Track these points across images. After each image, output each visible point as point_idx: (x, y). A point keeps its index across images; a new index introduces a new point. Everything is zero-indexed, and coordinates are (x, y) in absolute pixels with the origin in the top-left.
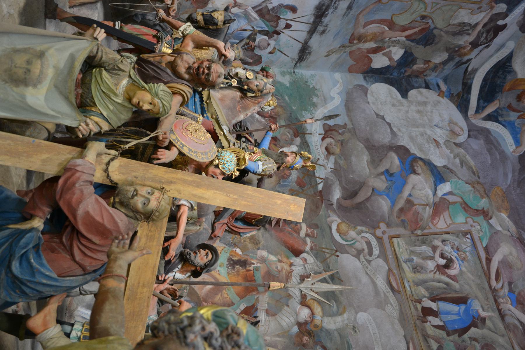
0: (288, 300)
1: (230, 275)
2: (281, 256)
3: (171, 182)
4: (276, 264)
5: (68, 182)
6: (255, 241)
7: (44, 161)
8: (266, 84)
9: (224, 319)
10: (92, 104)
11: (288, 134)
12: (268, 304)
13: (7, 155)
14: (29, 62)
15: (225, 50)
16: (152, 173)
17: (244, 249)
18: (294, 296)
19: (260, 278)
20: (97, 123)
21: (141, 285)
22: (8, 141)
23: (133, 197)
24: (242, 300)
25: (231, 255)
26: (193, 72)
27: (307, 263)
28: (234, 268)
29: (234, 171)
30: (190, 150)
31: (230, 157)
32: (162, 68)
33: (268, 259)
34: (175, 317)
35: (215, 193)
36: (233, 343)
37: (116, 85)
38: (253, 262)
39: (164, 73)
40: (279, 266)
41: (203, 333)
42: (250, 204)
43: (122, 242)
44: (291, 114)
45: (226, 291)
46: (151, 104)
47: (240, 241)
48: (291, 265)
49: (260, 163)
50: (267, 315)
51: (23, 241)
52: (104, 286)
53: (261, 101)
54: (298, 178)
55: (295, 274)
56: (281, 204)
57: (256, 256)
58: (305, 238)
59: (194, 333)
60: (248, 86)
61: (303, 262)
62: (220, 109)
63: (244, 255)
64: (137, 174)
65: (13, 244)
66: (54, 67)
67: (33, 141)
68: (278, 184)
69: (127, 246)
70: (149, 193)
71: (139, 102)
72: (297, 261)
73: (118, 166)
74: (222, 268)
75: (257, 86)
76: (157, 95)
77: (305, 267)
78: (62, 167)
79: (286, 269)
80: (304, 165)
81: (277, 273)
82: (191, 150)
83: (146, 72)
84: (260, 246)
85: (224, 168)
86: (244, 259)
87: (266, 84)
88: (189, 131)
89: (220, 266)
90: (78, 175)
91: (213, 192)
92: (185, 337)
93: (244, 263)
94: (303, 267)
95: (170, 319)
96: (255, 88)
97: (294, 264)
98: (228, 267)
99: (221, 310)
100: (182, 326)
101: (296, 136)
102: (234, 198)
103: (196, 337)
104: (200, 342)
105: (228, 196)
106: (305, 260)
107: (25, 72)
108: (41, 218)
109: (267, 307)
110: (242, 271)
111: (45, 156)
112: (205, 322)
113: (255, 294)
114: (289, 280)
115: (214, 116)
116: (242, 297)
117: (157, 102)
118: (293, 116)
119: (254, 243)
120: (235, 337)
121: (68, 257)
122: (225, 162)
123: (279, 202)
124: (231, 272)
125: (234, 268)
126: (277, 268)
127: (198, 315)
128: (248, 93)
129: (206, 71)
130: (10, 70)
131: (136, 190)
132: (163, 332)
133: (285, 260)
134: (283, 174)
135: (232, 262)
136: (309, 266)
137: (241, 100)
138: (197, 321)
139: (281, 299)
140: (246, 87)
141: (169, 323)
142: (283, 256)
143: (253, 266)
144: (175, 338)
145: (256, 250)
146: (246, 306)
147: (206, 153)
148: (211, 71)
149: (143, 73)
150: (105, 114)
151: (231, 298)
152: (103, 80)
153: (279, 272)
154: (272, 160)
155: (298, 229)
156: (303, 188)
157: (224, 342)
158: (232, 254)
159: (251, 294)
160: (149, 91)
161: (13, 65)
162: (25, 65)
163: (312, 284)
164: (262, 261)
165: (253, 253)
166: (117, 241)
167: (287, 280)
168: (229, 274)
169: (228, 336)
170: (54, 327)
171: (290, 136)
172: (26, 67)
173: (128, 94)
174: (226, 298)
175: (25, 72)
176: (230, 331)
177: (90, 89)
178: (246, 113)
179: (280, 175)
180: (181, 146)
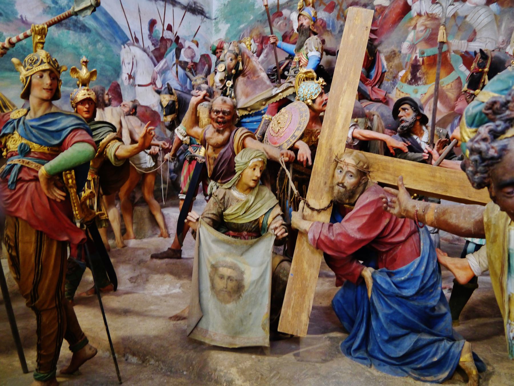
0: (459, 17)
1: (427, 82)
2: (409, 27)
3: (330, 149)
5: (330, 246)
6: (391, 56)
7: (310, 266)
8: (229, 51)
9: (476, 115)
10: (256, 223)
11: (279, 23)
12: (461, 39)
13: (305, 296)
14: (222, 277)
15: (199, 95)
16: (321, 168)
17: (400, 68)
19: (432, 49)
20: (274, 219)
21: (432, 179)
22: (292, 295)
23: (344, 187)
24: (455, 68)
25: (406, 81)
28: (420, 79)
29: (319, 83)
30: (298, 129)
31: (304, 88)
32: (219, 157)
33: (412, 41)
34: (469, 166)
35: (341, 106)
36: (504, 109)
37: (238, 201)
38: (414, 58)
39: (225, 155)
40: (420, 28)
41: (489, 141)
43: (389, 203)
44: (258, 21)
45: (444, 87)
46: (254, 169)
47: (391, 73)
48: (419, 15)
49: (310, 54)
50: (475, 41)
51: (384, 285)
52: (432, 223)
53: (247, 55)
54: (325, 10)
55: (431, 9)
57: (407, 55)
59: (488, 149)
60: (232, 69)
62: (256, 97)
63: (406, 67)
64: (322, 182)
66: (224, 256)
67: (292, 275)
68: (331, 33)
69: (394, 199)
70: (341, 172)
71: (253, 180)
72: (415, 8)
73: (314, 200)
74: (419, 91)
75: (231, 60)
78: (315, 251)
79: (424, 21)
80: (311, 5)
81: (428, 30)
83: (224, 172)
84: (397, 50)
85: (316, 94)
86: (410, 68)
87: (229, 51)
89: (417, 92)
90: (323, 238)
91: (340, 108)
92: (492, 158)
93: (415, 67)
95: (472, 172)
96: (234, 62)
97: (418, 11)
98: (418, 85)
99: (466, 118)
100: (479, 161)
101: (279, 14)
102: (347, 85)
103: (493, 148)
104: (498, 144)
105: (345, 92)
108: (362, 270)
109: (466, 41)
110: (423, 69)
111: (305, 266)
112: (478, 138)
113: (450, 55)
114: (437, 17)
115: (264, 103)
116: (451, 69)
117: (253, 163)
118: (260, 19)
119: (394, 58)
120: (497, 106)
121: (400, 247)
122: (309, 93)
123: (352, 37)
124: (424, 81)
126: (422, 31)
127: (469, 144)
128: (239, 69)
131: (338, 184)
132: (485, 178)
133: (413, 22)
134: (321, 27)
135: (413, 81)
137: (246, 75)
138: (477, 146)
139: (457, 25)
140: (233, 71)
141: (475, 173)
142: (409, 25)
143: (418, 58)
144: (491, 168)
145: (401, 55)
146: (462, 64)
148: (220, 110)
149: (225, 174)
150: (265, 211)
151: (452, 81)
152: (234, 213)
153: (426, 28)
154: (307, 41)
155: (380, 8)
156: (336, 4)
157: (501, 117)
158: (404, 80)
159: (449, 59)
161: (225, 290)
164: (414, 48)
165: (404, 58)
166: (388, 209)
167: (436, 19)
168: (425, 84)
169: (495, 113)
170: (469, 261)
171: (281, 22)
172: (226, 279)
173: (246, 190)
175: (231, 280)
176: (489, 111)
177: (242, 225)
178: (259, 71)
179: (322, 30)
180: (294, 138)
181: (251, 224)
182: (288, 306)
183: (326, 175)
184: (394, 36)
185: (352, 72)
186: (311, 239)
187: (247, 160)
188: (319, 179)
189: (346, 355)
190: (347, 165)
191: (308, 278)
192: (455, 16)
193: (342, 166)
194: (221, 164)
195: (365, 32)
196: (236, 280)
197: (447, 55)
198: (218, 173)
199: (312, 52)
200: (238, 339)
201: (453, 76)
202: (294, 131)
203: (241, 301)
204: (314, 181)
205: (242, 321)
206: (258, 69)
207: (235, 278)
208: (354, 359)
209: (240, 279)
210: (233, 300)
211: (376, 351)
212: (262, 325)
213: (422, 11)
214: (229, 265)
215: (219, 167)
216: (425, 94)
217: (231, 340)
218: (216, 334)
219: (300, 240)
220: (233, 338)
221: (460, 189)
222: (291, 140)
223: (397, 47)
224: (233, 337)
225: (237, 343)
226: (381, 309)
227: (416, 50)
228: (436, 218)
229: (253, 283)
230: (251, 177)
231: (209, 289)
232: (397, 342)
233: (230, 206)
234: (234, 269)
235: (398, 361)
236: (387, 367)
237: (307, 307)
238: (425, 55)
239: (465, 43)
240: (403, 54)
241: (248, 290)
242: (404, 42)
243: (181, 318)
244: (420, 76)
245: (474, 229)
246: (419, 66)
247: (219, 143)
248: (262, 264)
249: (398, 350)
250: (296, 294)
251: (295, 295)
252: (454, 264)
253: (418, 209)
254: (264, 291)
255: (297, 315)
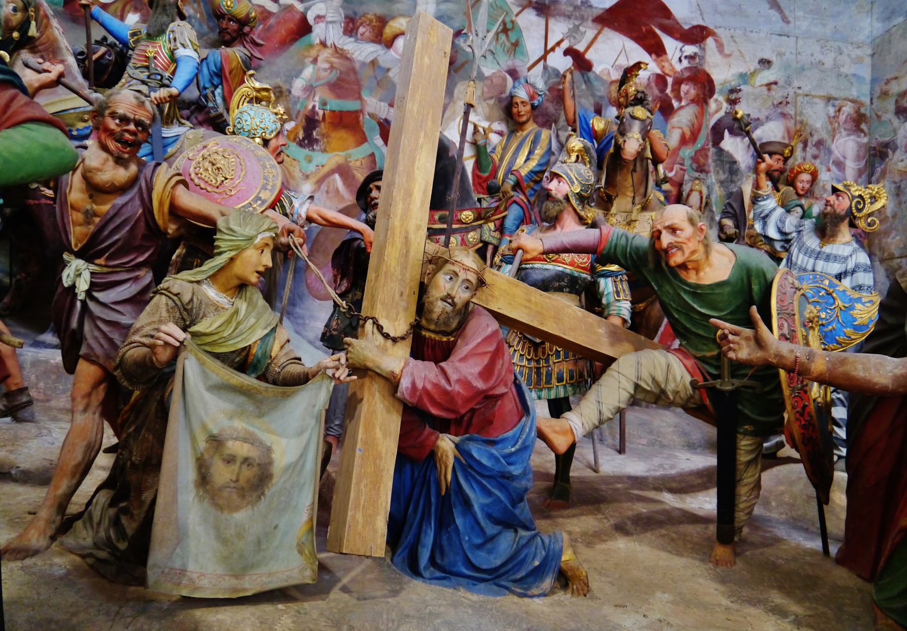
0: (379, 67)
1: (328, 149)
2: (306, 57)
3: (406, 238)
4: (318, 69)
5: (439, 400)
7: (385, 434)
10: (244, 354)
12: (381, 100)
13: (379, 487)
14: (230, 460)
18: (374, 56)
19: (338, 101)
20: (282, 347)
21: (527, 304)
22: (362, 487)
23: (453, 304)
24: (369, 139)
26: (127, 153)
27: (324, 17)
28: (317, 141)
29: (276, 114)
30: (264, 188)
31: (252, 115)
32: (112, 213)
33: (310, 80)
35: (418, 168)
37: (218, 308)
38: (310, 107)
39: (124, 210)
42: (431, 112)
45: (350, 162)
46: (262, 252)
48: (323, 44)
49: (181, 52)
51: (485, 461)
53: (44, 12)
55: (341, 42)
56: (430, 58)
57: (301, 100)
58: (280, 5)
60: (13, 29)
61: (323, 22)
62: (60, 101)
63: (297, 118)
64: (397, 291)
65: (487, 473)
66: (231, 418)
67: (360, 450)
70: (451, 278)
71: (257, 272)
72: (318, 32)
73: (387, 321)
76: (251, 239)
77: (331, 22)
78: (391, 408)
81: (334, 72)
82: (263, 185)
83: (120, 243)
84: (285, 87)
85: (272, 131)
86: (304, 121)
88: (223, 181)
89: (310, 161)
91: (416, 172)
93: (311, 122)
94: (330, 26)
97: (323, 39)
98: (313, 150)
106: (319, 18)
107: (249, 465)
108: (437, 438)
109: (386, 105)
110: (323, 128)
111: (379, 434)
114: (349, 56)
115: (86, 117)
117: (262, 239)
121: (499, 402)
122: (262, 126)
123: (426, 60)
124: (323, 147)
125: (317, 141)
126: (325, 70)
128: (30, 34)
129: (132, 127)
130: (243, 489)
131: (443, 300)
133: (313, 53)
135: (306, 142)
136: (331, 15)
139: (376, 78)
142: (306, 54)
143: (317, 108)
145: (291, 97)
146: (379, 136)
147: (259, 159)
148: (132, 116)
150: (230, 332)
151: (362, 156)
152: (214, 332)
153: (332, 67)
154: (172, 25)
155: (262, 13)
158: (292, 137)
159: (361, 123)
160: (240, 250)
161: (232, 485)
162: (235, 467)
163: (477, 35)
164: (311, 92)
165: (295, 103)
168: (324, 151)
170: (570, 422)
172: (238, 463)
173: (230, 289)
174: (362, 164)
175: (249, 465)
178: (65, 50)
180: (259, 202)
181: (235, 355)
182: (357, 507)
183: (401, 279)
184: (282, 62)
185: (430, 118)
186: (407, 388)
187: (253, 233)
188: (392, 285)
189: (412, 578)
190: (467, 269)
191: (383, 455)
192: (374, 63)
193: (456, 268)
194: (111, 226)
195: (444, 60)
196: (259, 465)
197: (359, 116)
198: (101, 243)
199: (186, 50)
200: (247, 578)
201: (365, 149)
202: (256, 188)
203: (263, 504)
204: (385, 288)
205: (259, 542)
206: (63, 46)
207: (257, 461)
208: (428, 581)
209: (267, 461)
210: (248, 503)
211: (460, 564)
212: (298, 545)
213: (327, 39)
214: (241, 435)
215: (106, 233)
216: (323, 166)
217: (234, 582)
218: (203, 575)
219: (369, 389)
220: (237, 579)
221: (555, 322)
222: (255, 206)
223: (286, 82)
224: (237, 577)
225: (247, 586)
226: (477, 500)
227: (314, 97)
228: (829, 369)
229: (286, 469)
230: (256, 266)
231: (192, 486)
232: (489, 546)
233: (203, 318)
234: (252, 444)
235: (490, 575)
236: (482, 586)
237: (384, 504)
238: (328, 107)
239: (384, 107)
240: (294, 97)
241: (278, 481)
242: (296, 78)
243: (31, 553)
244: (317, 137)
245: (893, 385)
246: (317, 121)
247: (117, 184)
248: (300, 433)
249: (492, 557)
250: (367, 484)
251: (366, 486)
252: (551, 427)
253: (798, 354)
254: (302, 481)
255: (370, 520)
